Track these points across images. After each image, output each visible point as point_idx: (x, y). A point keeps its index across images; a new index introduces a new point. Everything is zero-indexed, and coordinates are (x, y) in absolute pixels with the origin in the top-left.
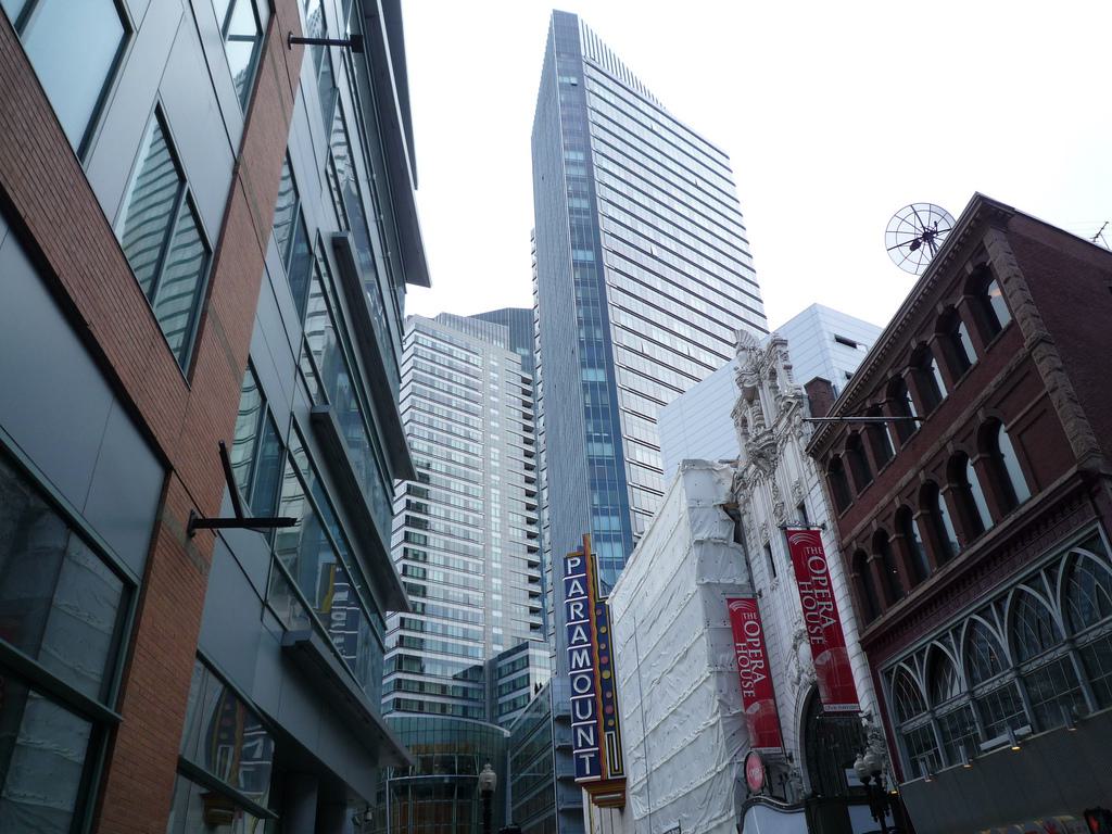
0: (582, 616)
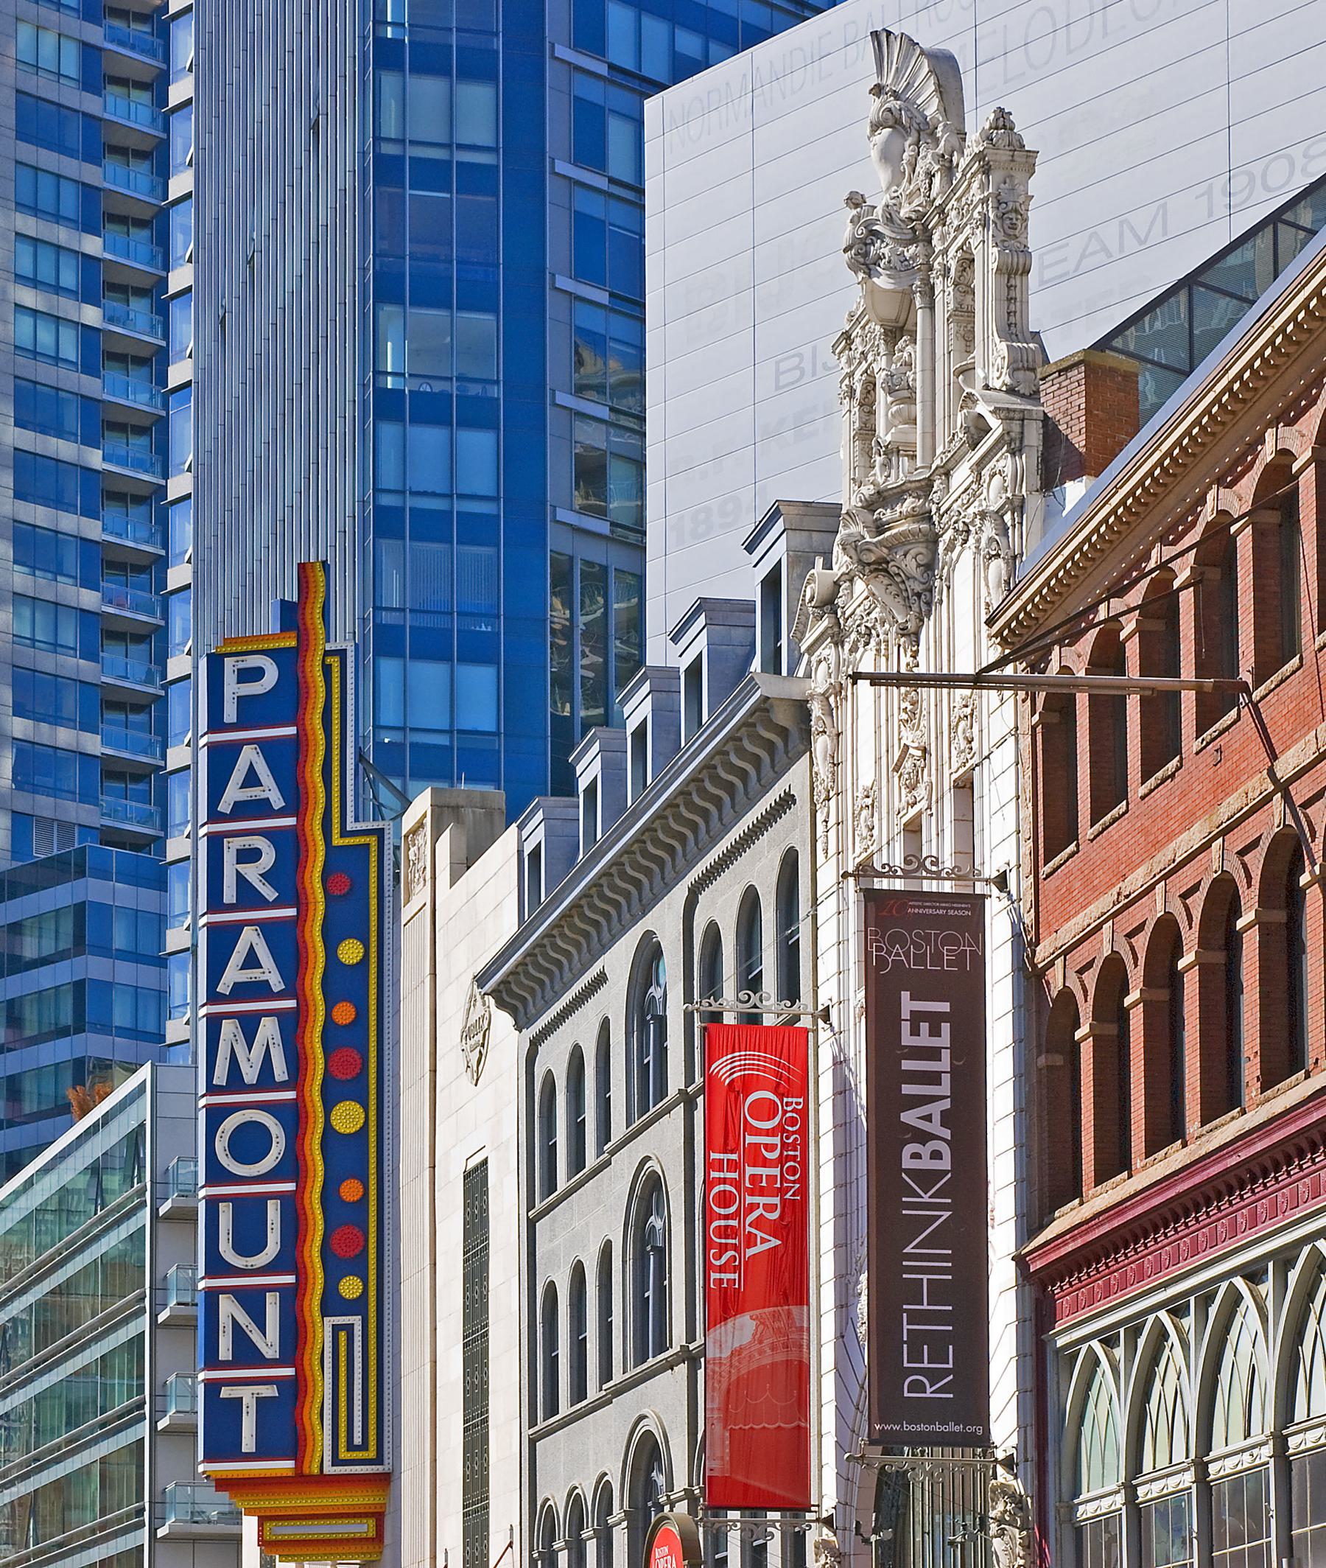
0: (270, 893)
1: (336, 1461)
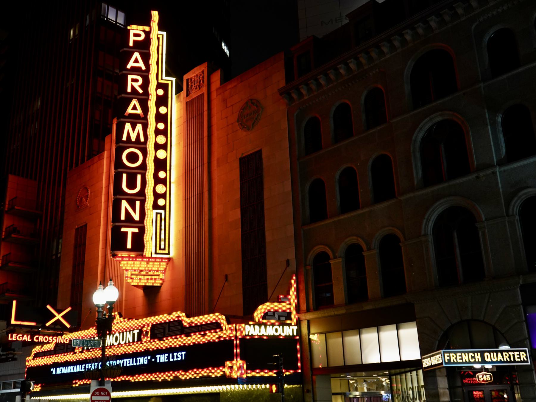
1: (156, 253)
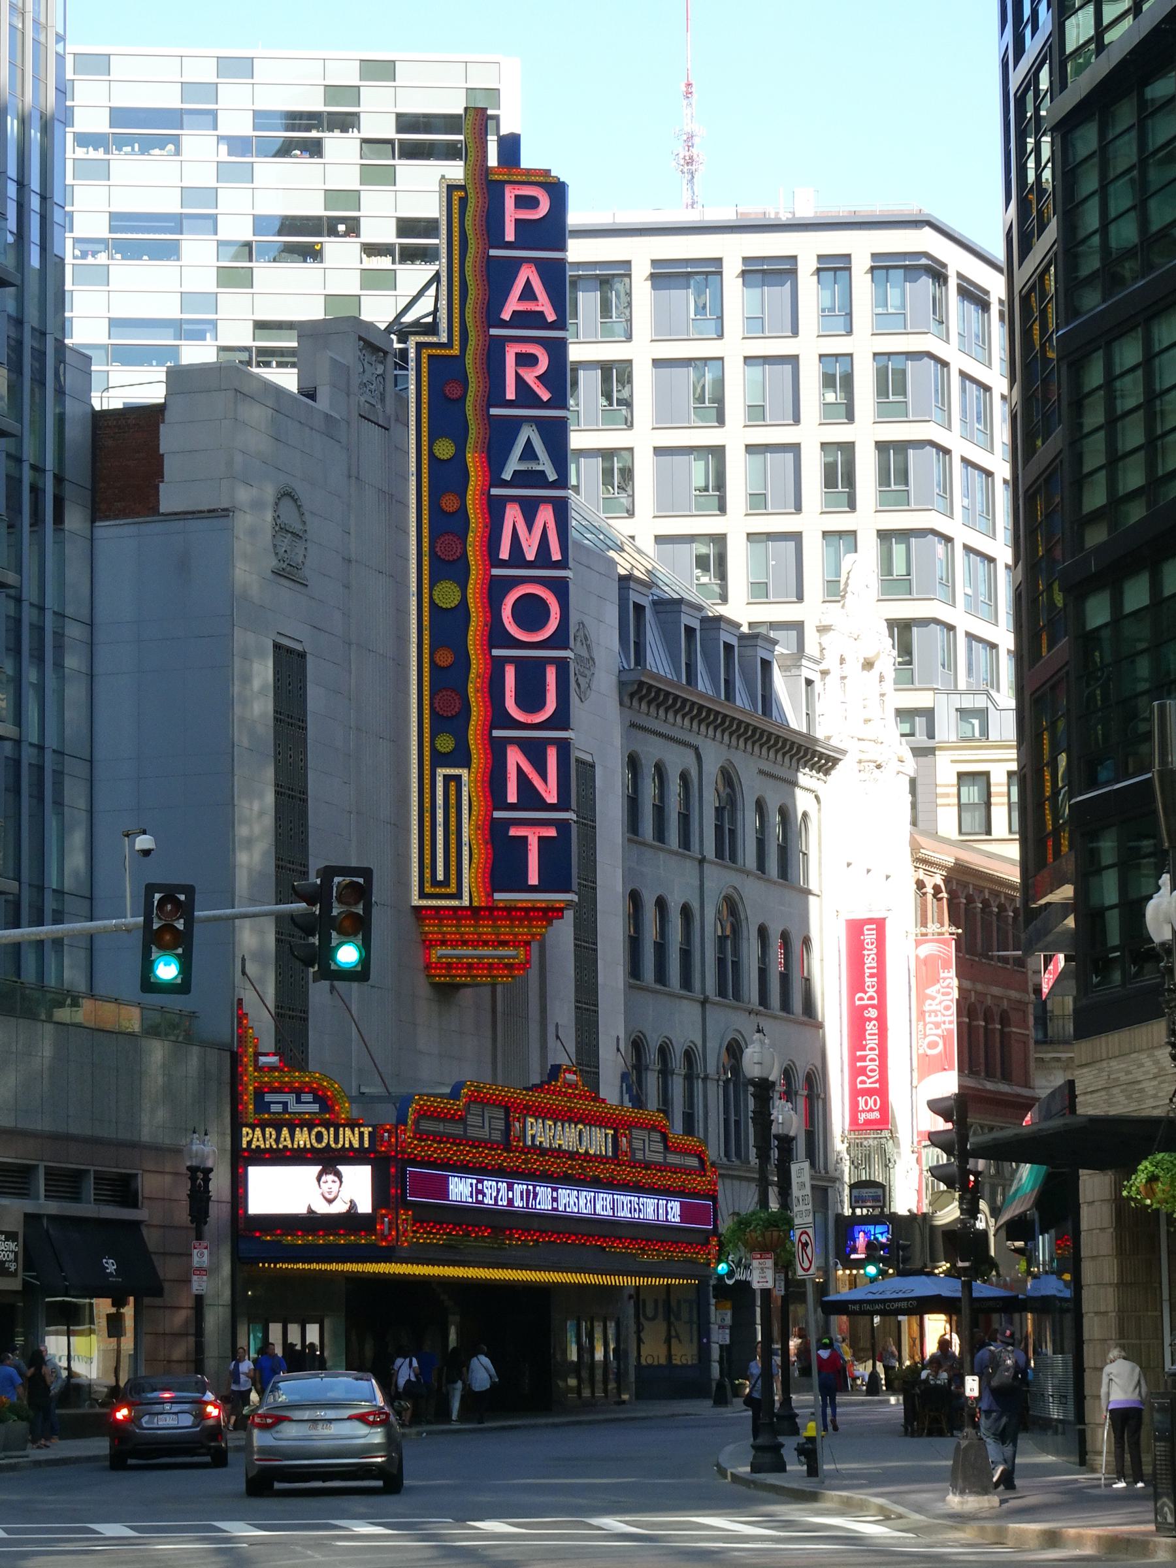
0: (545, 396)
